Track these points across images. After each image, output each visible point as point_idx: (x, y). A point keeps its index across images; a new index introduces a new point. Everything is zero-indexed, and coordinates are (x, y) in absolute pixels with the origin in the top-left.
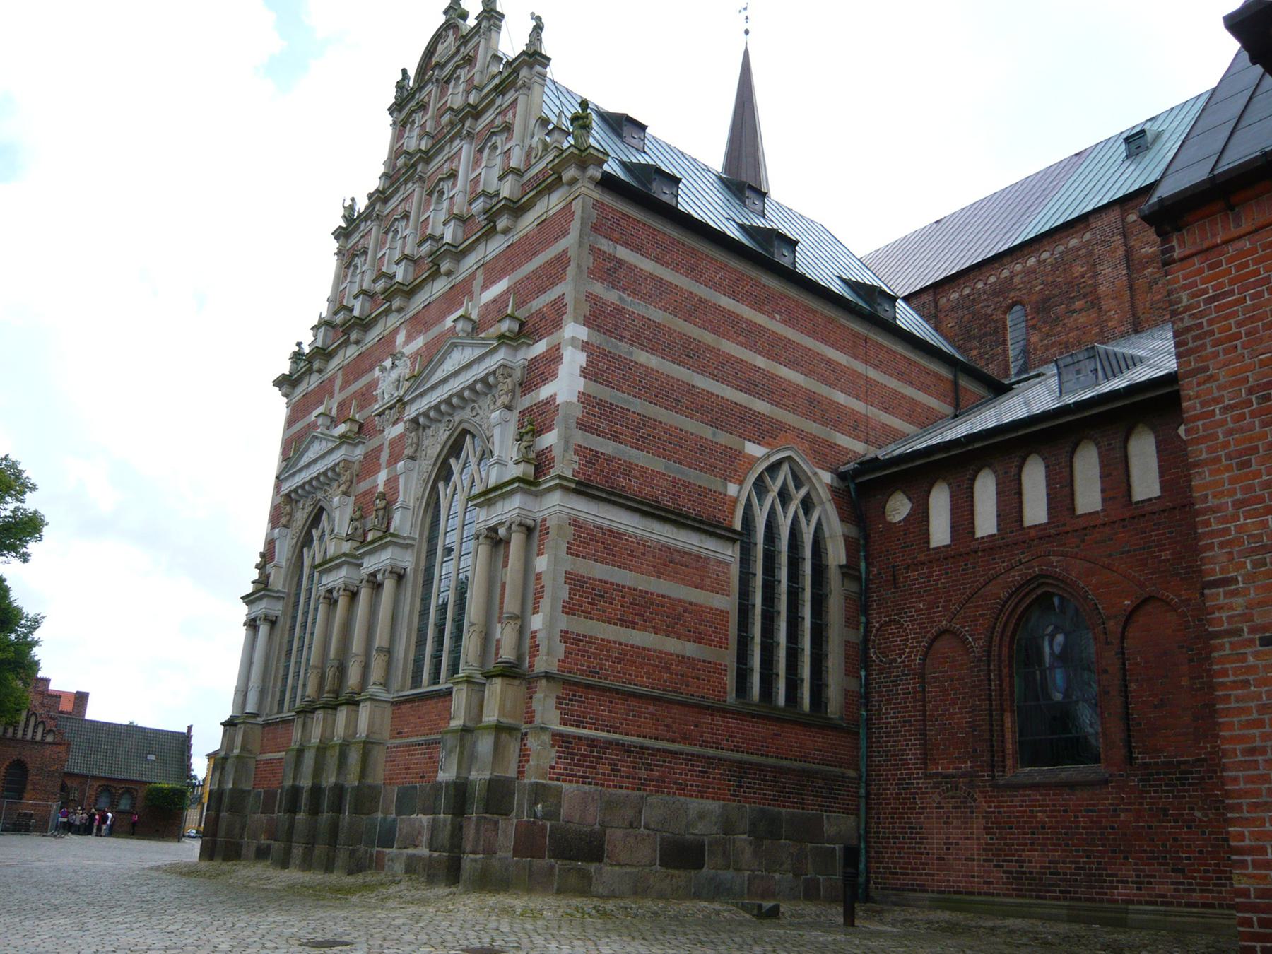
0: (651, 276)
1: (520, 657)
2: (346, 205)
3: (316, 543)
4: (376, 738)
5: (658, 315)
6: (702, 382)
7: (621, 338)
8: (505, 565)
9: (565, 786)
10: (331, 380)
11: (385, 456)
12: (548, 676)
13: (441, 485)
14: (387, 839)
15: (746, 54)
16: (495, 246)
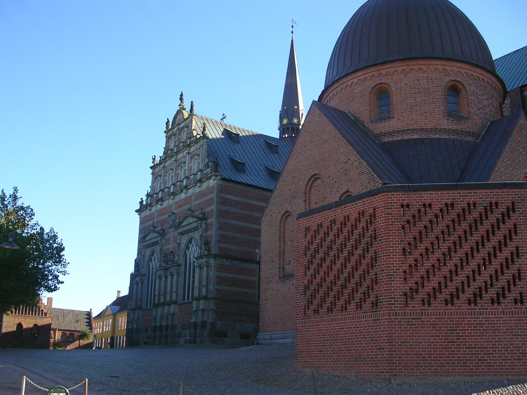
0: (235, 201)
1: (207, 294)
2: (153, 158)
3: (153, 261)
4: (175, 313)
5: (237, 210)
6: (248, 225)
7: (228, 218)
8: (203, 273)
9: (218, 322)
10: (153, 213)
11: (172, 240)
12: (213, 299)
13: (187, 251)
14: (179, 336)
15: (292, 40)
16: (197, 190)
